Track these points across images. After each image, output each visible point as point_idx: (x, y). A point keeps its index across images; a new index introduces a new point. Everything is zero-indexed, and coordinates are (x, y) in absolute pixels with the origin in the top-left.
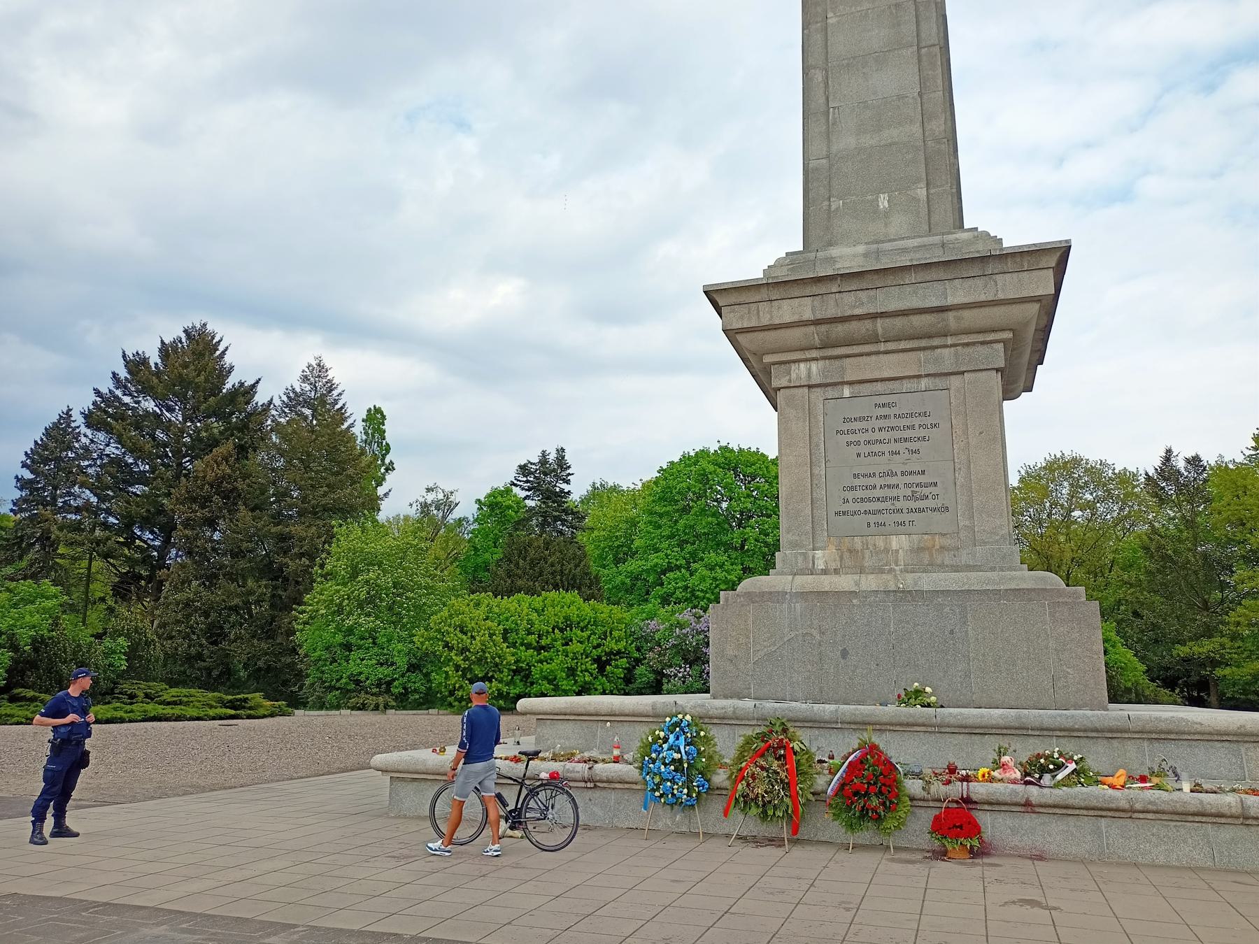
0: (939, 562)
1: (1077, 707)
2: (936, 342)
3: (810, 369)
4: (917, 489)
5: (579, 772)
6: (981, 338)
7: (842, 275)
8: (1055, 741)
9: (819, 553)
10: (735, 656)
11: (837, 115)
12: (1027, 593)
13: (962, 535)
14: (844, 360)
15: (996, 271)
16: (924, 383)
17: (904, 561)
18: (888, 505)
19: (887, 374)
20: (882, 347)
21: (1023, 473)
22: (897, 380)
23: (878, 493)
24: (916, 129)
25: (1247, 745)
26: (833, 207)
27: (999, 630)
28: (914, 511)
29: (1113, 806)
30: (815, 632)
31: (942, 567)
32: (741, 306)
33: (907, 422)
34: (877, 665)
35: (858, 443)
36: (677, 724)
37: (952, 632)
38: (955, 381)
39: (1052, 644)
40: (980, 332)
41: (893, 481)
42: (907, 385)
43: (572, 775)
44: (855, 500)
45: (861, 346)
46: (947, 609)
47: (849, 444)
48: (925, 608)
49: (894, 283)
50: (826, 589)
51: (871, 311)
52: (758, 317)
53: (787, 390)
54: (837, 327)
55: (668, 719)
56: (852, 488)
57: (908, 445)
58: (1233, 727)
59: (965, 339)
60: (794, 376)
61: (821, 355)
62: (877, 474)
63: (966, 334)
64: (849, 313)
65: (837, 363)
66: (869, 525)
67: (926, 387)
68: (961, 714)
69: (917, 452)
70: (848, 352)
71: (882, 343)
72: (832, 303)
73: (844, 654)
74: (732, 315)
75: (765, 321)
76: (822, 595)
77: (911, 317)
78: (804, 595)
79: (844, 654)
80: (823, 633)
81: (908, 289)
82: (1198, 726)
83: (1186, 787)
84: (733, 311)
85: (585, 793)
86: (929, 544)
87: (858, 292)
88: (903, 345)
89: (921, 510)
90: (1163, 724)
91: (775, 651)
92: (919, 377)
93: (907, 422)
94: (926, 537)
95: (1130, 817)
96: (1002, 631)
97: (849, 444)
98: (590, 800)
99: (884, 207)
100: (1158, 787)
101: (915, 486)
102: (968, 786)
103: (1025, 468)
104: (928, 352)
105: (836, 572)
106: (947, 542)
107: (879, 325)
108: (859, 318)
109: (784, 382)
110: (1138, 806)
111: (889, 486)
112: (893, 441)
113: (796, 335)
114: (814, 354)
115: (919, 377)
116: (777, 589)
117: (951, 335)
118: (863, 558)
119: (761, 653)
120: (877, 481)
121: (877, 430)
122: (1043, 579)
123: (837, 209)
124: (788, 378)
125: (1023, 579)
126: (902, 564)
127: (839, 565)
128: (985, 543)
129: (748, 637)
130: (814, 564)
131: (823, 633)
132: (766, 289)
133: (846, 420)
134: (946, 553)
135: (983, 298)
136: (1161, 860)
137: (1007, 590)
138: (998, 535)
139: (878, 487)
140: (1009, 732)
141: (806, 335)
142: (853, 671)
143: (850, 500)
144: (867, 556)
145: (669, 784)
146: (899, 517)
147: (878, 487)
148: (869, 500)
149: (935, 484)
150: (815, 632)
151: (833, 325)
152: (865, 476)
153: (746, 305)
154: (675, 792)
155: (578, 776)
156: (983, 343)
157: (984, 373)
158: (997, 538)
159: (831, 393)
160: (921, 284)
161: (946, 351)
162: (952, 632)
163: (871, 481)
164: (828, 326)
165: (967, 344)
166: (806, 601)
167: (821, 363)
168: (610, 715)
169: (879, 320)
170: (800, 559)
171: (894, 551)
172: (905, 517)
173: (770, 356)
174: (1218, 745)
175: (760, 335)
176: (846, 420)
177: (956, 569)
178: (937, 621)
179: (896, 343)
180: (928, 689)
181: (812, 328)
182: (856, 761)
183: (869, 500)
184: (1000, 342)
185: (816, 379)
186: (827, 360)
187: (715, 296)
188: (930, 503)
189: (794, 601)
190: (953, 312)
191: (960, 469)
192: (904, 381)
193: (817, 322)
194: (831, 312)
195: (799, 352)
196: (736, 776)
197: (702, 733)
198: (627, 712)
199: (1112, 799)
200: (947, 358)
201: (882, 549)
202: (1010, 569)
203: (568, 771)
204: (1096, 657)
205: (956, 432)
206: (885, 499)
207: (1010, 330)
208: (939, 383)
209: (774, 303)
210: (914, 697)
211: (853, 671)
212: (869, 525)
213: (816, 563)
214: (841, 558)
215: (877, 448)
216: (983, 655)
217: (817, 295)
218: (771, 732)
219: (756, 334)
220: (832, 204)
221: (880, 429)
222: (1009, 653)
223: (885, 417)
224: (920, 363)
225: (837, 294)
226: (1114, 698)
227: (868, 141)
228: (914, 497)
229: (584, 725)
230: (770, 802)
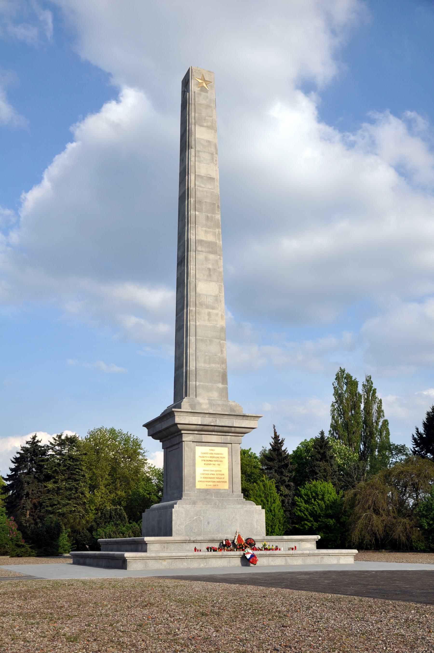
2: (227, 434)
35: (205, 461)
44: (204, 478)
47: (202, 460)
56: (203, 474)
66: (207, 485)
73: (208, 523)
79: (208, 523)
89: (219, 482)
97: (202, 460)
123: (198, 386)
128: (235, 492)
223: (212, 454)
227: (207, 366)
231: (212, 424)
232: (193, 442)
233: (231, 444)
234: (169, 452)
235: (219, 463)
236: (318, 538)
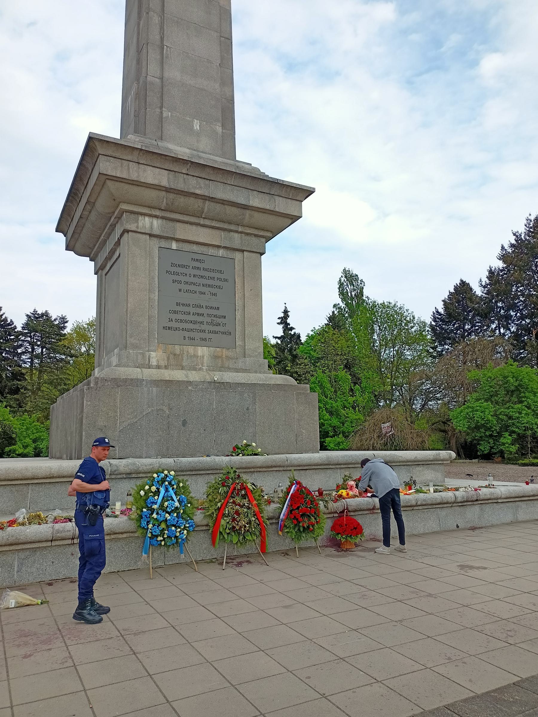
0: (226, 366)
1: (306, 452)
2: (233, 227)
3: (152, 223)
4: (214, 319)
5: (70, 531)
6: (256, 232)
7: (192, 163)
8: (339, 470)
9: (153, 354)
10: (105, 426)
11: (169, 53)
12: (283, 387)
13: (238, 350)
14: (175, 223)
15: (276, 194)
16: (221, 252)
17: (207, 364)
18: (197, 326)
19: (201, 240)
20: (202, 222)
21: (75, 325)
22: (206, 245)
23: (191, 318)
24: (217, 86)
25: (413, 467)
26: (165, 115)
27: (272, 408)
28: (212, 332)
29: (409, 504)
30: (165, 409)
31: (229, 369)
32: (116, 159)
33: (212, 275)
34: (205, 430)
35: (180, 282)
36: (163, 480)
37: (248, 409)
38: (238, 256)
39: (296, 416)
40: (256, 229)
41: (200, 311)
42: (211, 251)
43: (63, 535)
44: (177, 321)
45: (189, 216)
46: (246, 395)
47: (174, 281)
48: (234, 393)
49: (221, 181)
50: (167, 379)
51: (206, 194)
52: (129, 172)
53: (134, 234)
54: (180, 198)
55: (155, 475)
56: (175, 312)
57: (210, 289)
58: (413, 458)
59: (248, 231)
60: (140, 224)
61: (163, 215)
62: (191, 305)
63: (249, 227)
64: (192, 191)
65: (171, 224)
66: (185, 337)
67: (222, 255)
68: (300, 458)
69: (215, 295)
70: (181, 219)
71: (202, 219)
72: (181, 180)
73: (184, 423)
74: (108, 163)
75: (134, 176)
76: (169, 383)
77: (226, 206)
78: (157, 383)
79: (184, 423)
80: (171, 409)
81: (229, 187)
82: (400, 458)
83: (432, 490)
84: (109, 161)
85: (67, 549)
86: (220, 354)
87: (198, 178)
88: (214, 224)
89: (216, 332)
90: (388, 458)
91: (136, 422)
92: (219, 247)
93: (212, 275)
94: (218, 349)
95: (413, 510)
96: (273, 409)
97: (174, 281)
98: (72, 554)
99: (197, 129)
100: (418, 491)
101: (213, 317)
102: (346, 502)
103: (76, 322)
104: (226, 233)
105: (166, 367)
106: (230, 353)
107: (206, 205)
108: (196, 196)
109: (133, 227)
110: (419, 503)
111: (198, 314)
112: (201, 285)
113: (151, 195)
114: (157, 213)
115: (219, 247)
116: (132, 377)
117: (241, 226)
118: (182, 360)
119: (126, 424)
120: (192, 310)
121: (192, 276)
122: (286, 379)
123: (168, 117)
124: (136, 224)
125: (271, 378)
126: (206, 365)
127: (166, 364)
128: (250, 356)
129: (116, 412)
130: (149, 361)
131: (171, 409)
132: (138, 152)
133: (173, 265)
134: (231, 360)
135: (268, 207)
136: (422, 531)
137: (274, 384)
138: (257, 352)
139: (191, 314)
140: (321, 467)
141: (158, 197)
142: (189, 435)
143: (174, 320)
144: (184, 359)
145: (173, 528)
146: (203, 335)
147: (191, 314)
148: (186, 321)
149: (225, 317)
150: (165, 409)
151: (179, 196)
152: (184, 305)
153: (120, 160)
154: (178, 534)
155: (70, 534)
156: (256, 236)
157: (254, 254)
158: (257, 354)
159: (164, 244)
160: (236, 187)
161: (236, 235)
162: (248, 409)
163: (186, 309)
164: (175, 195)
165: (247, 234)
166: (158, 386)
167: (160, 221)
168: (44, 478)
169: (207, 201)
170: (140, 357)
171: (201, 357)
172: (207, 335)
173: (125, 204)
174: (403, 467)
175: (126, 186)
176: (173, 265)
177: (237, 370)
178: (240, 402)
179: (210, 221)
180: (254, 444)
181: (164, 193)
182: (295, 492)
183: (186, 321)
184: (264, 237)
185: (156, 231)
186: (164, 220)
187: (97, 143)
188: (221, 329)
189: (149, 386)
190: (249, 211)
191: (238, 310)
192: (210, 248)
193: (168, 190)
194: (180, 185)
195: (147, 208)
196: (216, 515)
197: (181, 485)
198: (65, 474)
199: (409, 500)
200: (236, 240)
201: (192, 354)
202: (264, 373)
203: (58, 531)
204: (316, 423)
205: (237, 287)
206: (195, 322)
207: (271, 232)
208: (230, 254)
209: (141, 166)
210: (236, 450)
211: (189, 435)
212: (185, 337)
213: (151, 361)
214: (168, 358)
215: (192, 288)
216: (263, 423)
217: (172, 171)
218: (228, 478)
219: (123, 184)
220: (163, 112)
221: (194, 276)
222: (276, 421)
224: (222, 238)
225: (185, 175)
226: (323, 448)
228: (211, 323)
229: (14, 489)
230: (248, 531)
231: (198, 192)
232: (151, 235)
233: (243, 251)
234: (106, 275)
235: (214, 291)
236: (450, 457)
